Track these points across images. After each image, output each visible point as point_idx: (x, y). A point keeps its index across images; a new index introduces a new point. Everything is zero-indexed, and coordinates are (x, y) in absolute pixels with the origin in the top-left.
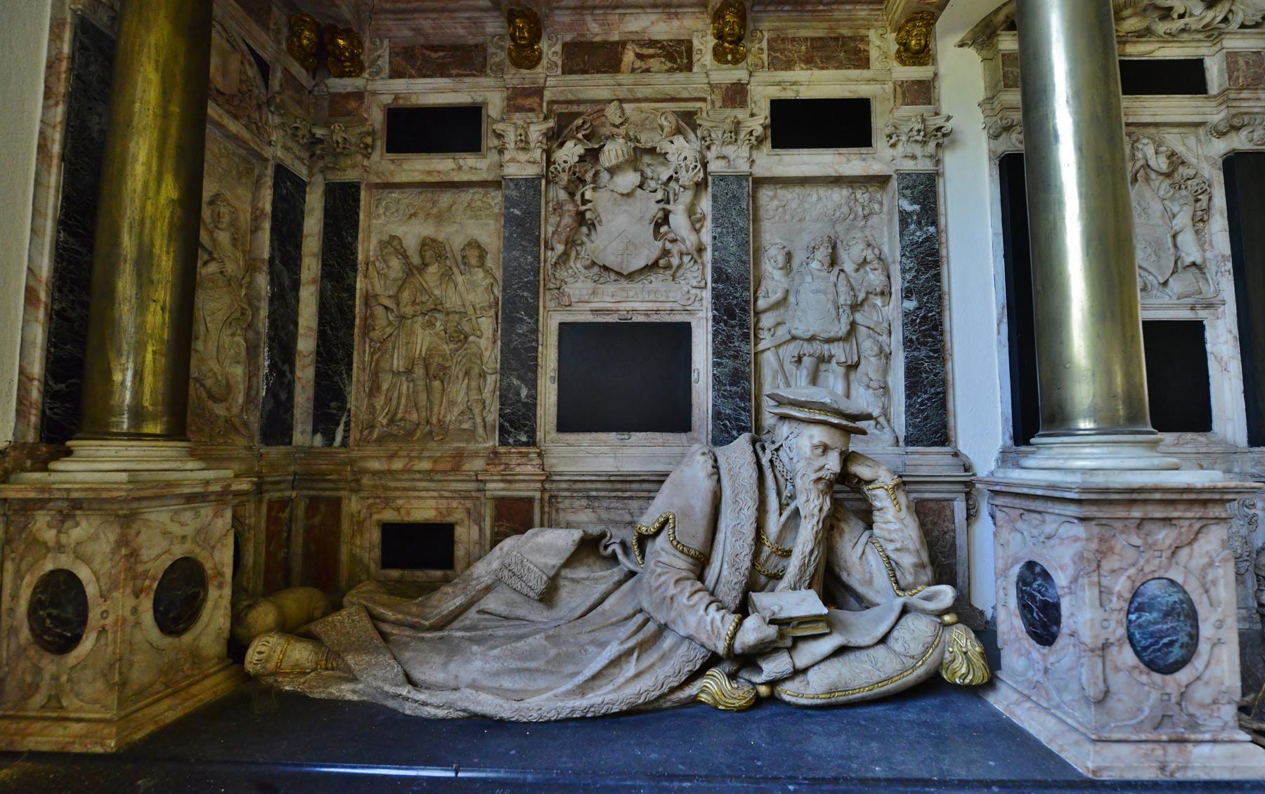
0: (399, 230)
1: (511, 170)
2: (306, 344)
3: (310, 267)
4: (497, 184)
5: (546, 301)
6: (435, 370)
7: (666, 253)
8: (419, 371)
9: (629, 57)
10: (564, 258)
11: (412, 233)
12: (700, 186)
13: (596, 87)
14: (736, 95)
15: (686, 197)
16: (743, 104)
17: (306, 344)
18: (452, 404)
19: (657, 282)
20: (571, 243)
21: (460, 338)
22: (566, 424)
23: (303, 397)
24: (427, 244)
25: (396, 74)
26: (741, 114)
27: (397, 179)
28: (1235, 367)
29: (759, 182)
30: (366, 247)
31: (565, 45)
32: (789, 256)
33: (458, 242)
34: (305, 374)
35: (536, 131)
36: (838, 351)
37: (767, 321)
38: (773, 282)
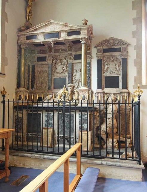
0: (38, 69)
1: (49, 63)
2: (30, 81)
3: (31, 73)
4: (48, 64)
5: (53, 76)
6: (42, 83)
7: (64, 71)
8: (41, 83)
9: (60, 51)
10: (54, 72)
11: (40, 69)
12: (67, 64)
13: (57, 54)
14: (71, 54)
15: (66, 65)
16: (71, 55)
17: (30, 81)
18: (44, 86)
19: (63, 74)
20: (55, 70)
21: (44, 80)
22: (54, 88)
23: (30, 85)
24: (41, 70)
25: (38, 54)
26: (71, 57)
27: (39, 64)
28: (121, 81)
29: (73, 63)
30: (35, 71)
31: (54, 50)
32: (76, 71)
33: (44, 70)
34: (30, 83)
35: (51, 59)
36: (80, 80)
37: (74, 77)
38: (75, 73)
